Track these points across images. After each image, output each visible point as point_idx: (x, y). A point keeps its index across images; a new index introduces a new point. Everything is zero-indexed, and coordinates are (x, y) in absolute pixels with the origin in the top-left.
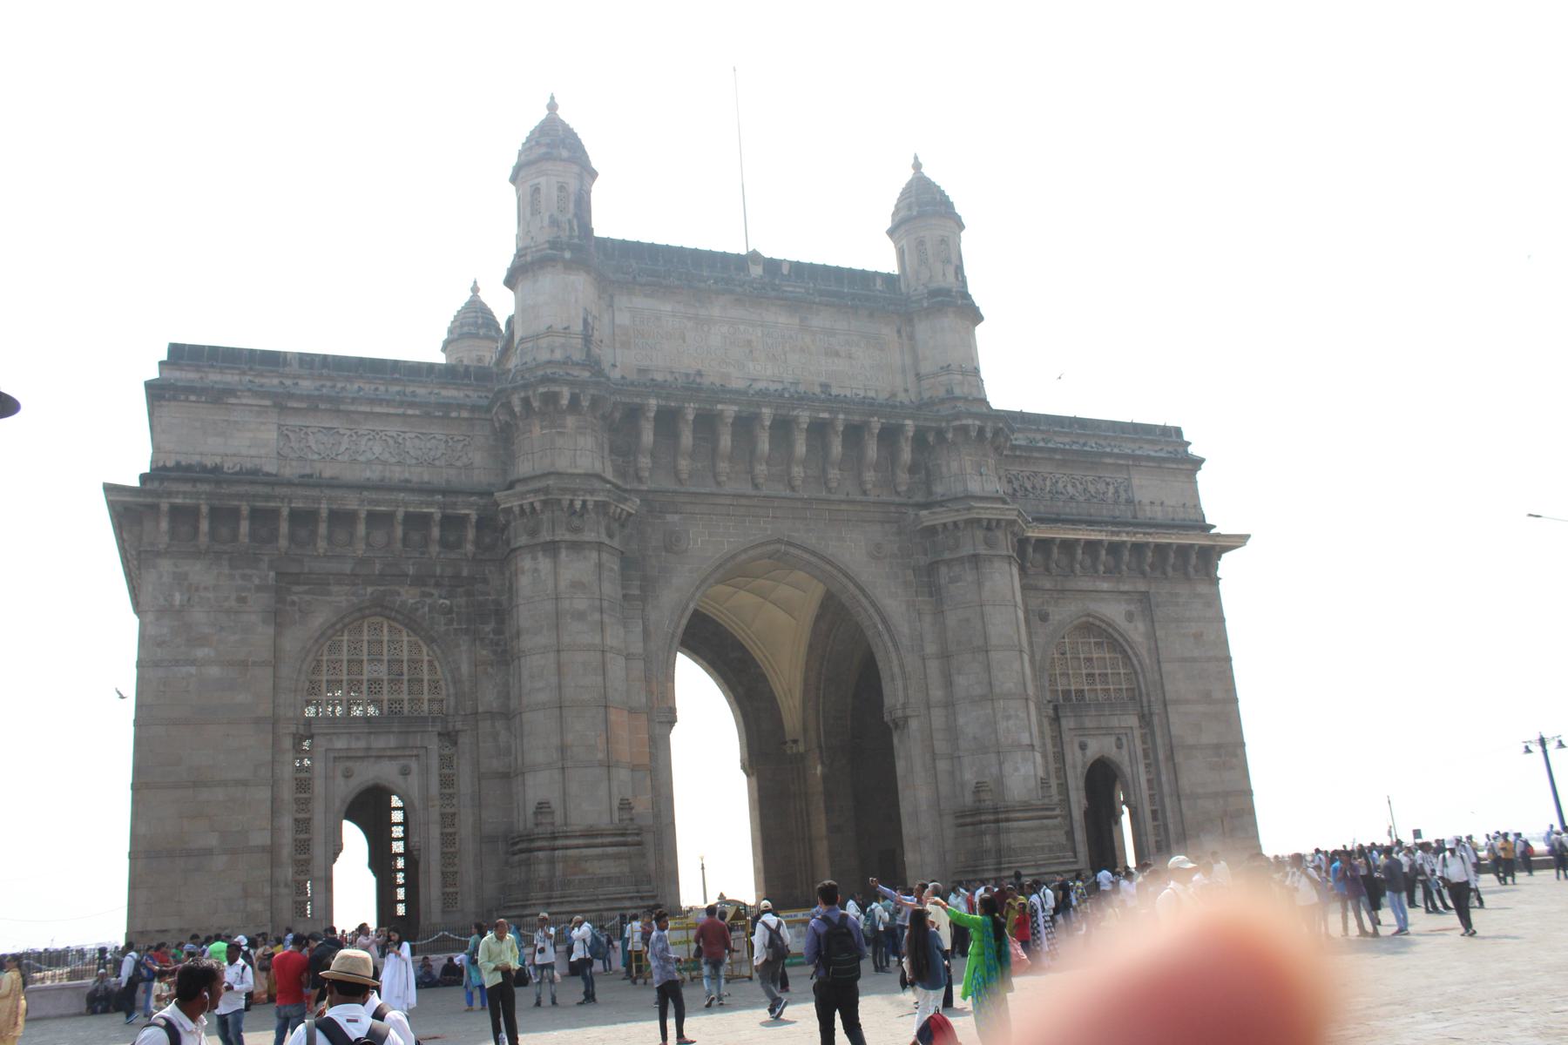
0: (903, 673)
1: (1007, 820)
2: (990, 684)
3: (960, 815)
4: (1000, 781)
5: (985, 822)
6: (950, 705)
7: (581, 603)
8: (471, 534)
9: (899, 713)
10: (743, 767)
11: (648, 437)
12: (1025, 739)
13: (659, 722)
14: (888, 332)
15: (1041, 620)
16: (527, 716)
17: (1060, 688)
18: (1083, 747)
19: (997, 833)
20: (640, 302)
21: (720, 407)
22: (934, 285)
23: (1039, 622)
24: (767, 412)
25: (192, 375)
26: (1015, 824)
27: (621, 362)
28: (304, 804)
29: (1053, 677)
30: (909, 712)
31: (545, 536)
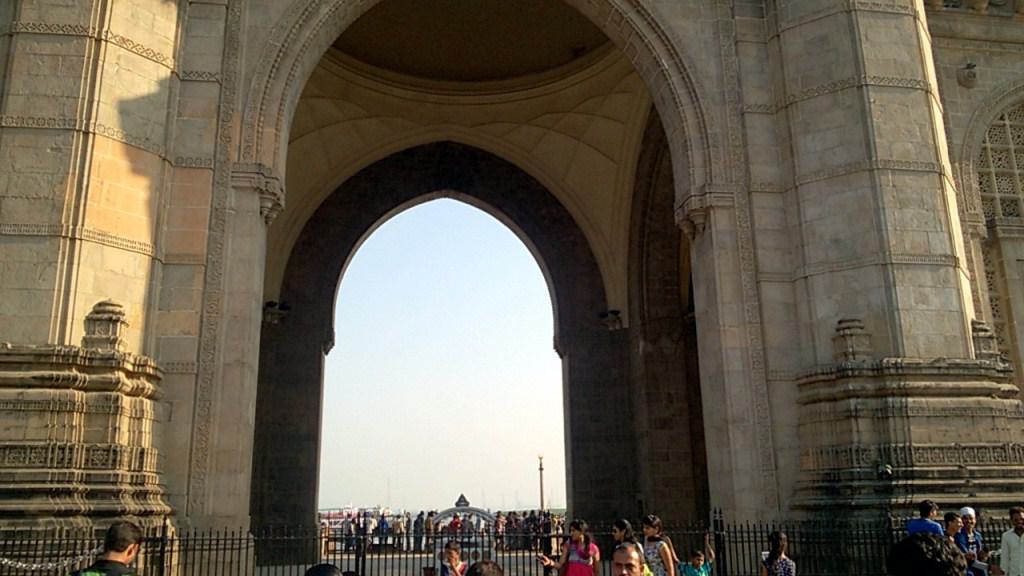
0: (704, 137)
1: (907, 393)
2: (868, 145)
3: (807, 381)
4: (889, 314)
5: (849, 395)
6: (789, 188)
9: (695, 203)
10: (556, 347)
13: (234, 187)
15: (960, 83)
17: (998, 196)
19: (882, 416)
23: (958, 88)
29: (986, 178)
30: (710, 200)
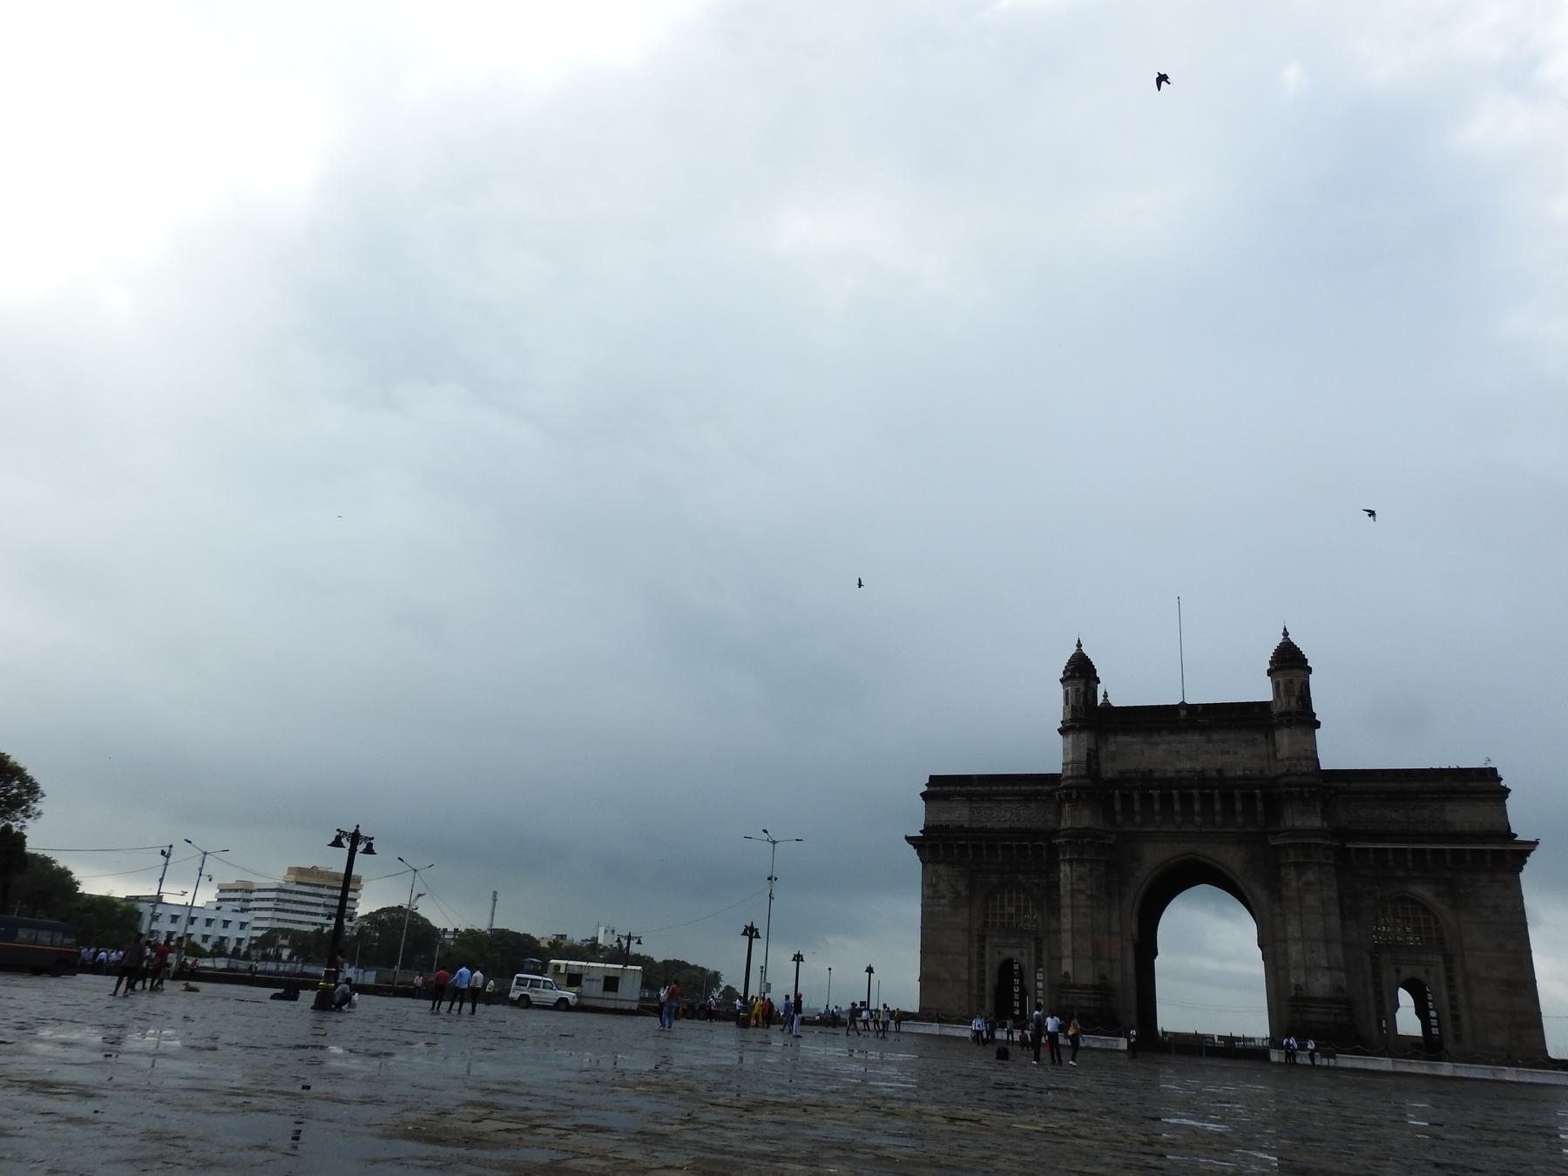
7: (1082, 886)
8: (1044, 853)
11: (1118, 807)
12: (1324, 963)
14: (1260, 737)
16: (1063, 934)
18: (1398, 971)
20: (1121, 738)
21: (1150, 792)
22: (1283, 709)
24: (1174, 792)
25: (938, 789)
26: (1313, 1009)
27: (1109, 770)
28: (982, 964)
31: (1068, 857)
